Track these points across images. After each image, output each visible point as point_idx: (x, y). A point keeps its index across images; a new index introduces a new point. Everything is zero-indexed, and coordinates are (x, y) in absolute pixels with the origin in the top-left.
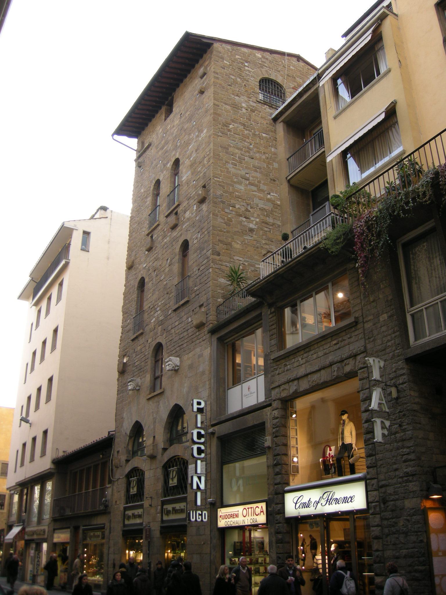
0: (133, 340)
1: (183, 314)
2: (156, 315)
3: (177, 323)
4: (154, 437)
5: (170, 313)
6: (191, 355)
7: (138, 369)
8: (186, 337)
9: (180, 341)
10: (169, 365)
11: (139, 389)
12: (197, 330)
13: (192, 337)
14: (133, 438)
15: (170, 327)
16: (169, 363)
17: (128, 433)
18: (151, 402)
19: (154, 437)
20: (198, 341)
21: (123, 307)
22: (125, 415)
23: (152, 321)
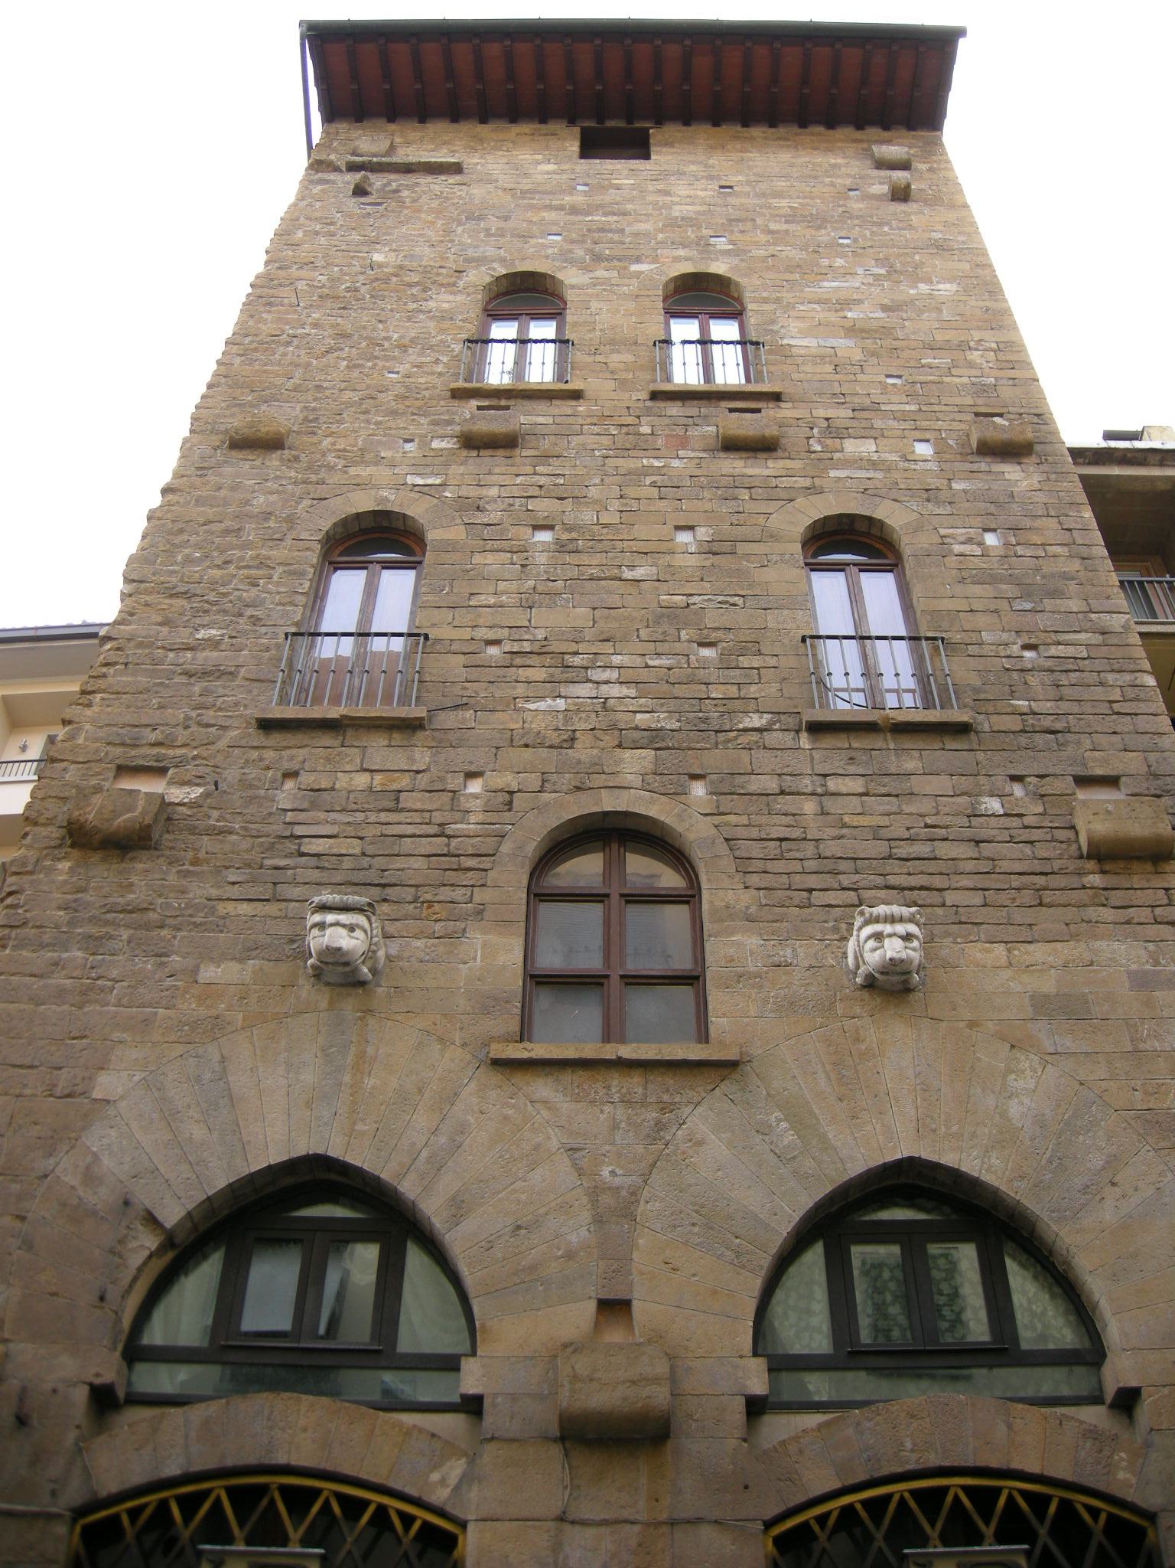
0: (267, 725)
1: (911, 764)
2: (583, 690)
3: (858, 785)
4: (613, 1308)
5: (756, 721)
6: (1038, 952)
7: (339, 878)
8: (970, 866)
9: (892, 866)
10: (907, 937)
11: (362, 984)
12: (1091, 865)
13: (1040, 881)
14: (170, 1255)
15: (772, 784)
16: (912, 928)
17: (172, 1215)
18: (543, 1087)
19: (613, 1308)
20: (1107, 914)
21: (132, 560)
22: (106, 1084)
23: (541, 705)
